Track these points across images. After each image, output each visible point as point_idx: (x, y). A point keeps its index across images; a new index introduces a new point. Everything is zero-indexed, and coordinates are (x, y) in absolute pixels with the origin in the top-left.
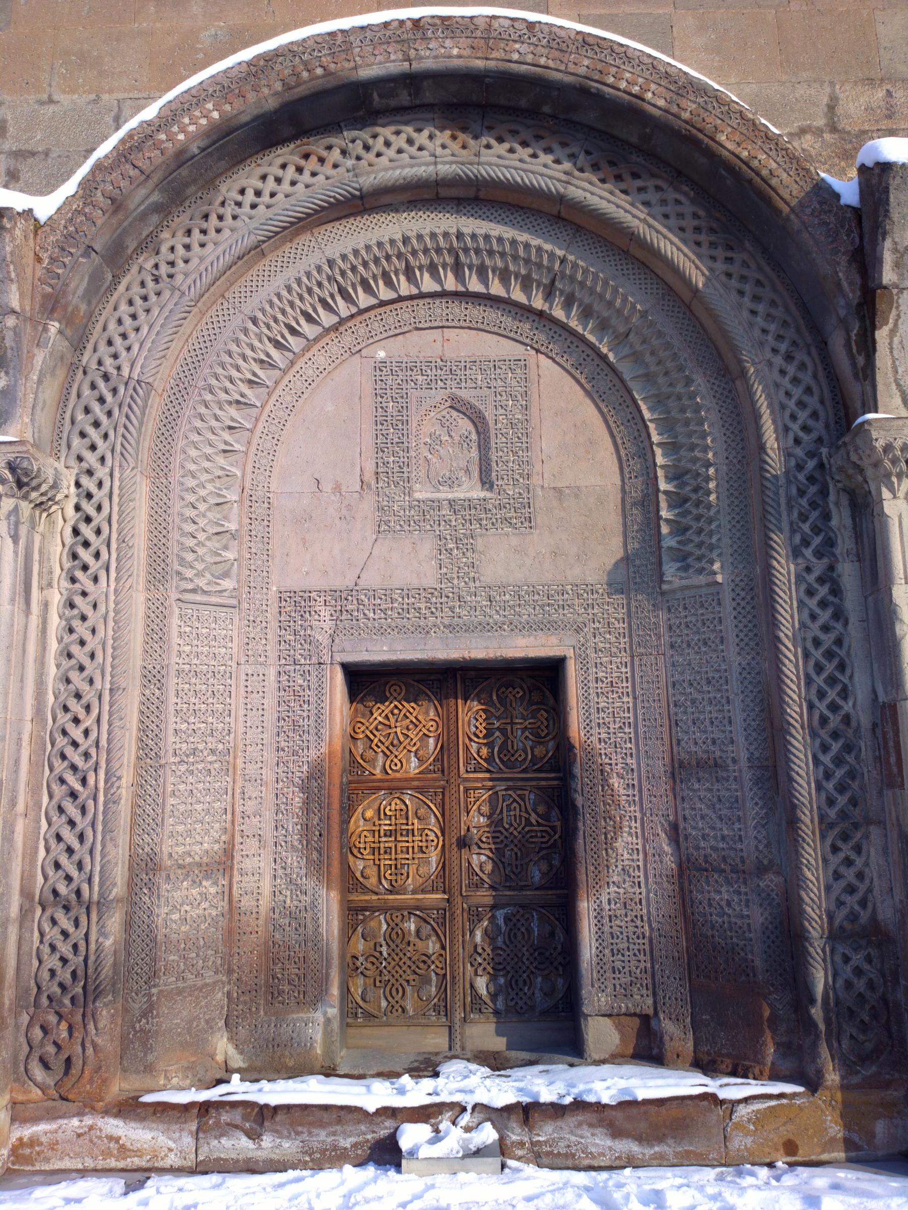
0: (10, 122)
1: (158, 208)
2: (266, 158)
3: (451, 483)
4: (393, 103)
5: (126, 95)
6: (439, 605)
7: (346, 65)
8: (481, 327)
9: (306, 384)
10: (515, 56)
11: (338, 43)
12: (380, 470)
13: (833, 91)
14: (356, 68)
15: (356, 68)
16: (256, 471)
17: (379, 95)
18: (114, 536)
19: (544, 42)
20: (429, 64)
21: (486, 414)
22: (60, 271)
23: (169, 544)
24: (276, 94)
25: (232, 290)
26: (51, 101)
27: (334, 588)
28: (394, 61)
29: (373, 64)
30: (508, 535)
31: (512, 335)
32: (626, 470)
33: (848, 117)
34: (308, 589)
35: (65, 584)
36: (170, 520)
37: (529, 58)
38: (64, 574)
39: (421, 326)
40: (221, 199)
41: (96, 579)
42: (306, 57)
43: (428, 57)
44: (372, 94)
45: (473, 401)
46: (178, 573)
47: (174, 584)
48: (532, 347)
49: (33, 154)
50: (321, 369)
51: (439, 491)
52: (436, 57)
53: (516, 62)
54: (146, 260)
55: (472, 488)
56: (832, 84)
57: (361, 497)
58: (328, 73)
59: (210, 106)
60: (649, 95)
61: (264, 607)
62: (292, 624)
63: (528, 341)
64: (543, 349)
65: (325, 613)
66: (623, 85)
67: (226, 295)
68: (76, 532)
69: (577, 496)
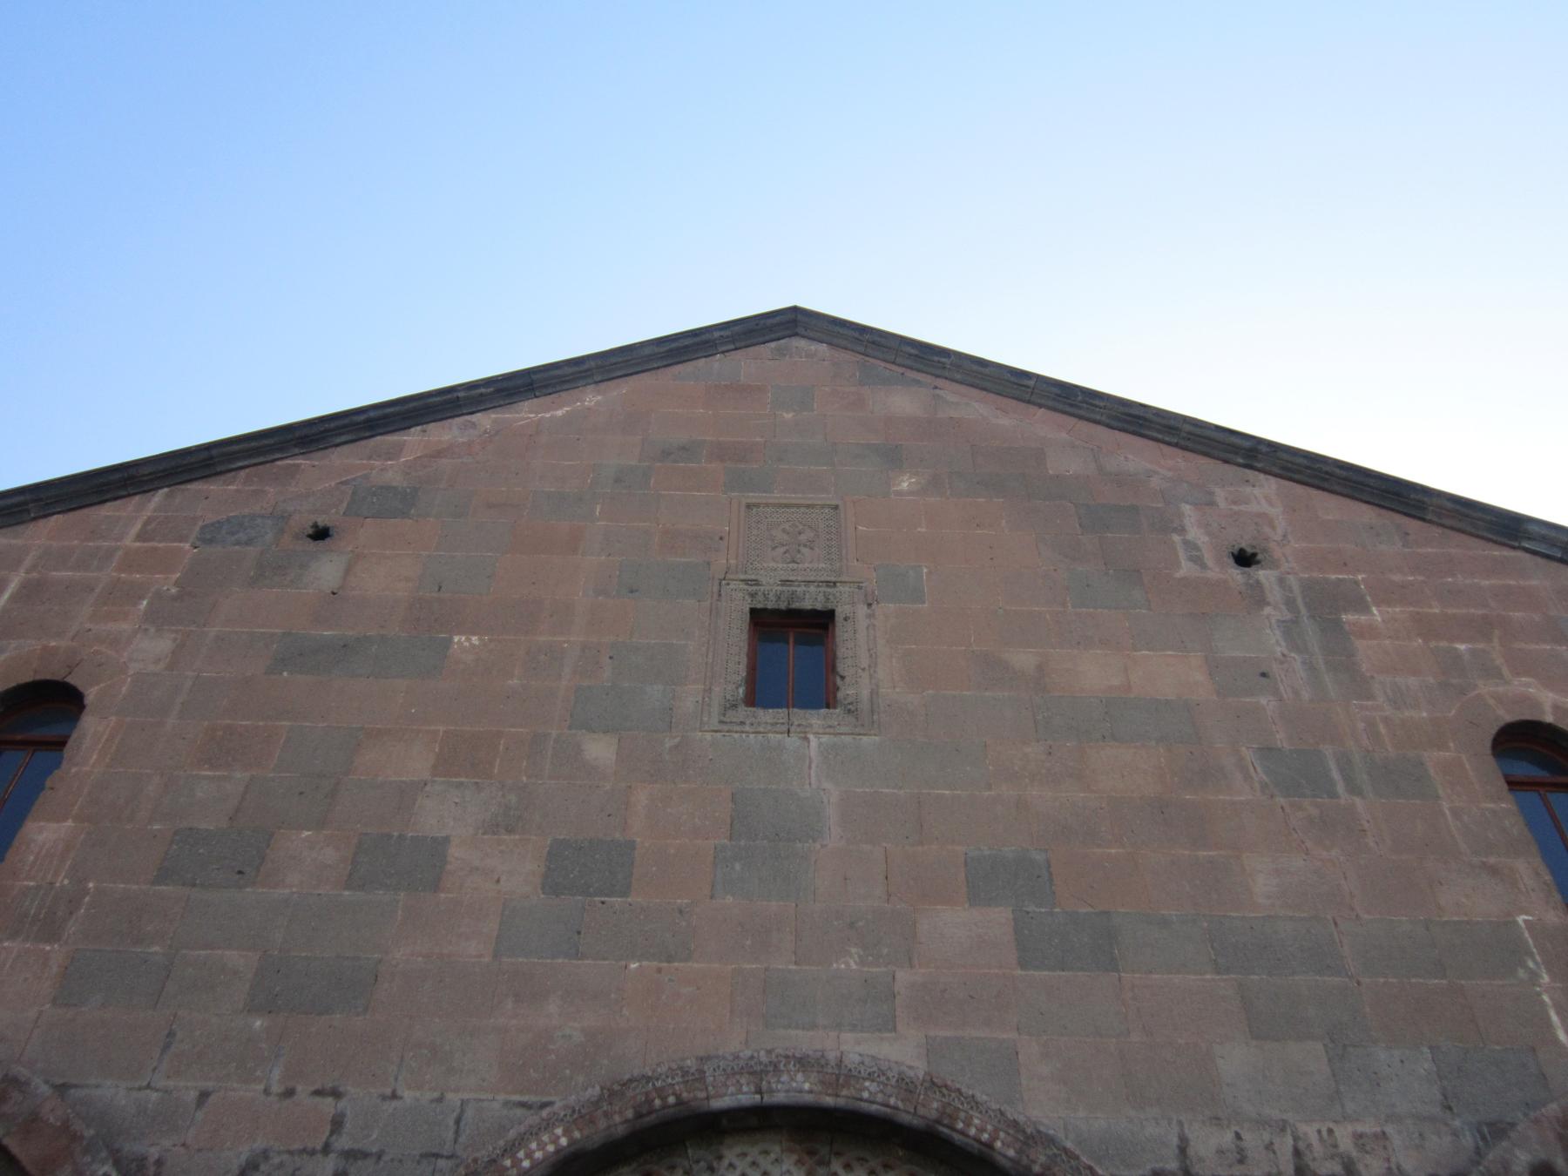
0: (348, 1113)
7: (702, 1095)
10: (866, 1095)
11: (692, 1070)
13: (1182, 1130)
14: (708, 1098)
15: (708, 1098)
19: (893, 1081)
20: (780, 1098)
24: (626, 1121)
26: (394, 1096)
28: (746, 1093)
29: (725, 1095)
33: (1201, 1160)
37: (880, 1098)
42: (659, 1084)
43: (779, 1091)
49: (366, 1155)
52: (787, 1091)
53: (866, 1101)
56: (1180, 1123)
58: (680, 1102)
59: (559, 1131)
60: (998, 1144)
66: (972, 1131)
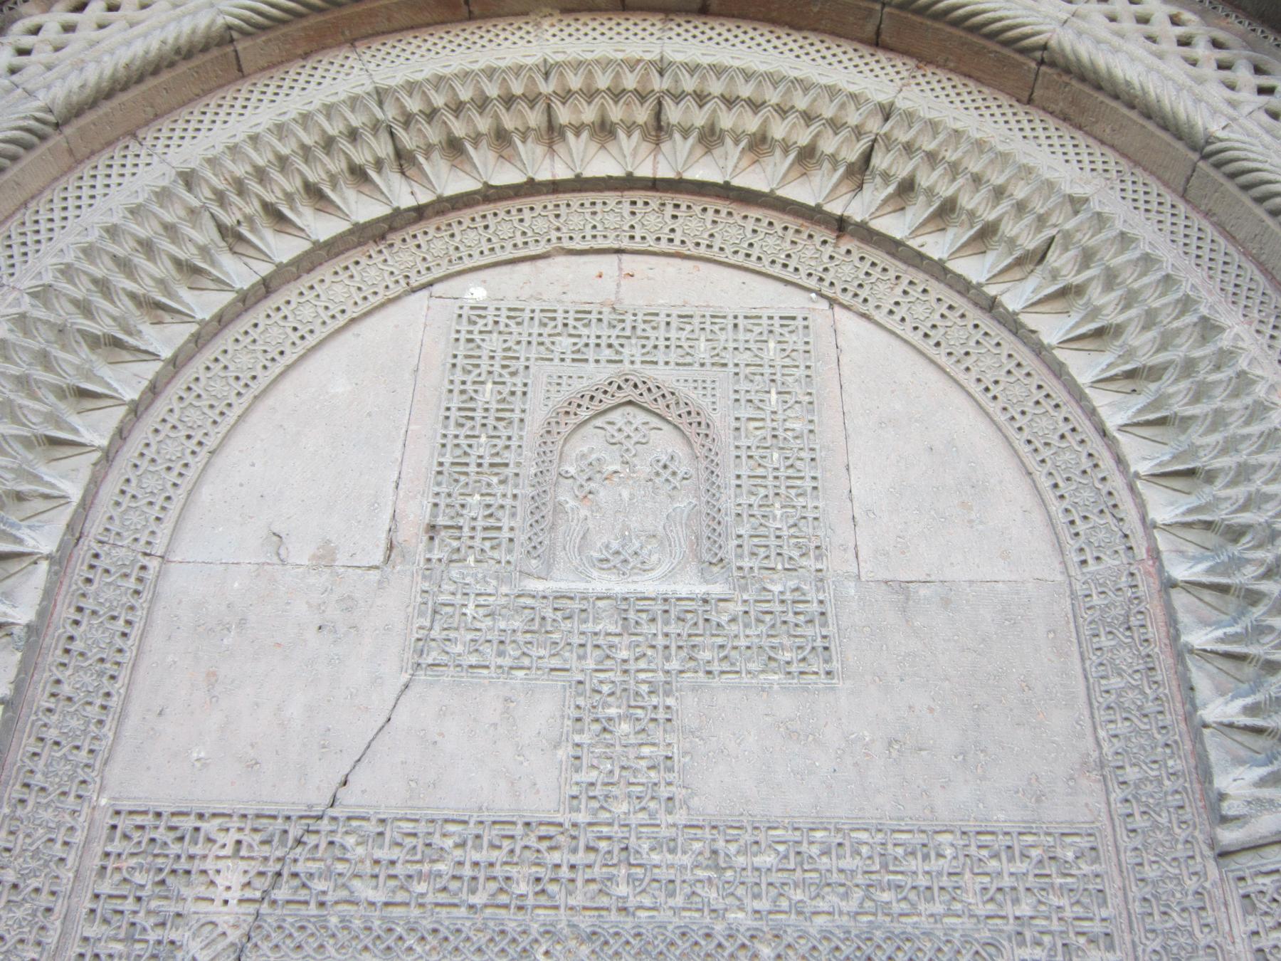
6: (565, 872)
8: (708, 254)
9: (294, 337)
12: (441, 521)
16: (126, 501)
21: (716, 417)
27: (269, 809)
31: (777, 270)
32: (1070, 545)
34: (197, 807)
45: (684, 390)
51: (588, 579)
55: (669, 576)
61: (58, 849)
62: (129, 905)
63: (812, 283)
64: (846, 299)
65: (231, 876)
67: (141, 134)
69: (946, 602)
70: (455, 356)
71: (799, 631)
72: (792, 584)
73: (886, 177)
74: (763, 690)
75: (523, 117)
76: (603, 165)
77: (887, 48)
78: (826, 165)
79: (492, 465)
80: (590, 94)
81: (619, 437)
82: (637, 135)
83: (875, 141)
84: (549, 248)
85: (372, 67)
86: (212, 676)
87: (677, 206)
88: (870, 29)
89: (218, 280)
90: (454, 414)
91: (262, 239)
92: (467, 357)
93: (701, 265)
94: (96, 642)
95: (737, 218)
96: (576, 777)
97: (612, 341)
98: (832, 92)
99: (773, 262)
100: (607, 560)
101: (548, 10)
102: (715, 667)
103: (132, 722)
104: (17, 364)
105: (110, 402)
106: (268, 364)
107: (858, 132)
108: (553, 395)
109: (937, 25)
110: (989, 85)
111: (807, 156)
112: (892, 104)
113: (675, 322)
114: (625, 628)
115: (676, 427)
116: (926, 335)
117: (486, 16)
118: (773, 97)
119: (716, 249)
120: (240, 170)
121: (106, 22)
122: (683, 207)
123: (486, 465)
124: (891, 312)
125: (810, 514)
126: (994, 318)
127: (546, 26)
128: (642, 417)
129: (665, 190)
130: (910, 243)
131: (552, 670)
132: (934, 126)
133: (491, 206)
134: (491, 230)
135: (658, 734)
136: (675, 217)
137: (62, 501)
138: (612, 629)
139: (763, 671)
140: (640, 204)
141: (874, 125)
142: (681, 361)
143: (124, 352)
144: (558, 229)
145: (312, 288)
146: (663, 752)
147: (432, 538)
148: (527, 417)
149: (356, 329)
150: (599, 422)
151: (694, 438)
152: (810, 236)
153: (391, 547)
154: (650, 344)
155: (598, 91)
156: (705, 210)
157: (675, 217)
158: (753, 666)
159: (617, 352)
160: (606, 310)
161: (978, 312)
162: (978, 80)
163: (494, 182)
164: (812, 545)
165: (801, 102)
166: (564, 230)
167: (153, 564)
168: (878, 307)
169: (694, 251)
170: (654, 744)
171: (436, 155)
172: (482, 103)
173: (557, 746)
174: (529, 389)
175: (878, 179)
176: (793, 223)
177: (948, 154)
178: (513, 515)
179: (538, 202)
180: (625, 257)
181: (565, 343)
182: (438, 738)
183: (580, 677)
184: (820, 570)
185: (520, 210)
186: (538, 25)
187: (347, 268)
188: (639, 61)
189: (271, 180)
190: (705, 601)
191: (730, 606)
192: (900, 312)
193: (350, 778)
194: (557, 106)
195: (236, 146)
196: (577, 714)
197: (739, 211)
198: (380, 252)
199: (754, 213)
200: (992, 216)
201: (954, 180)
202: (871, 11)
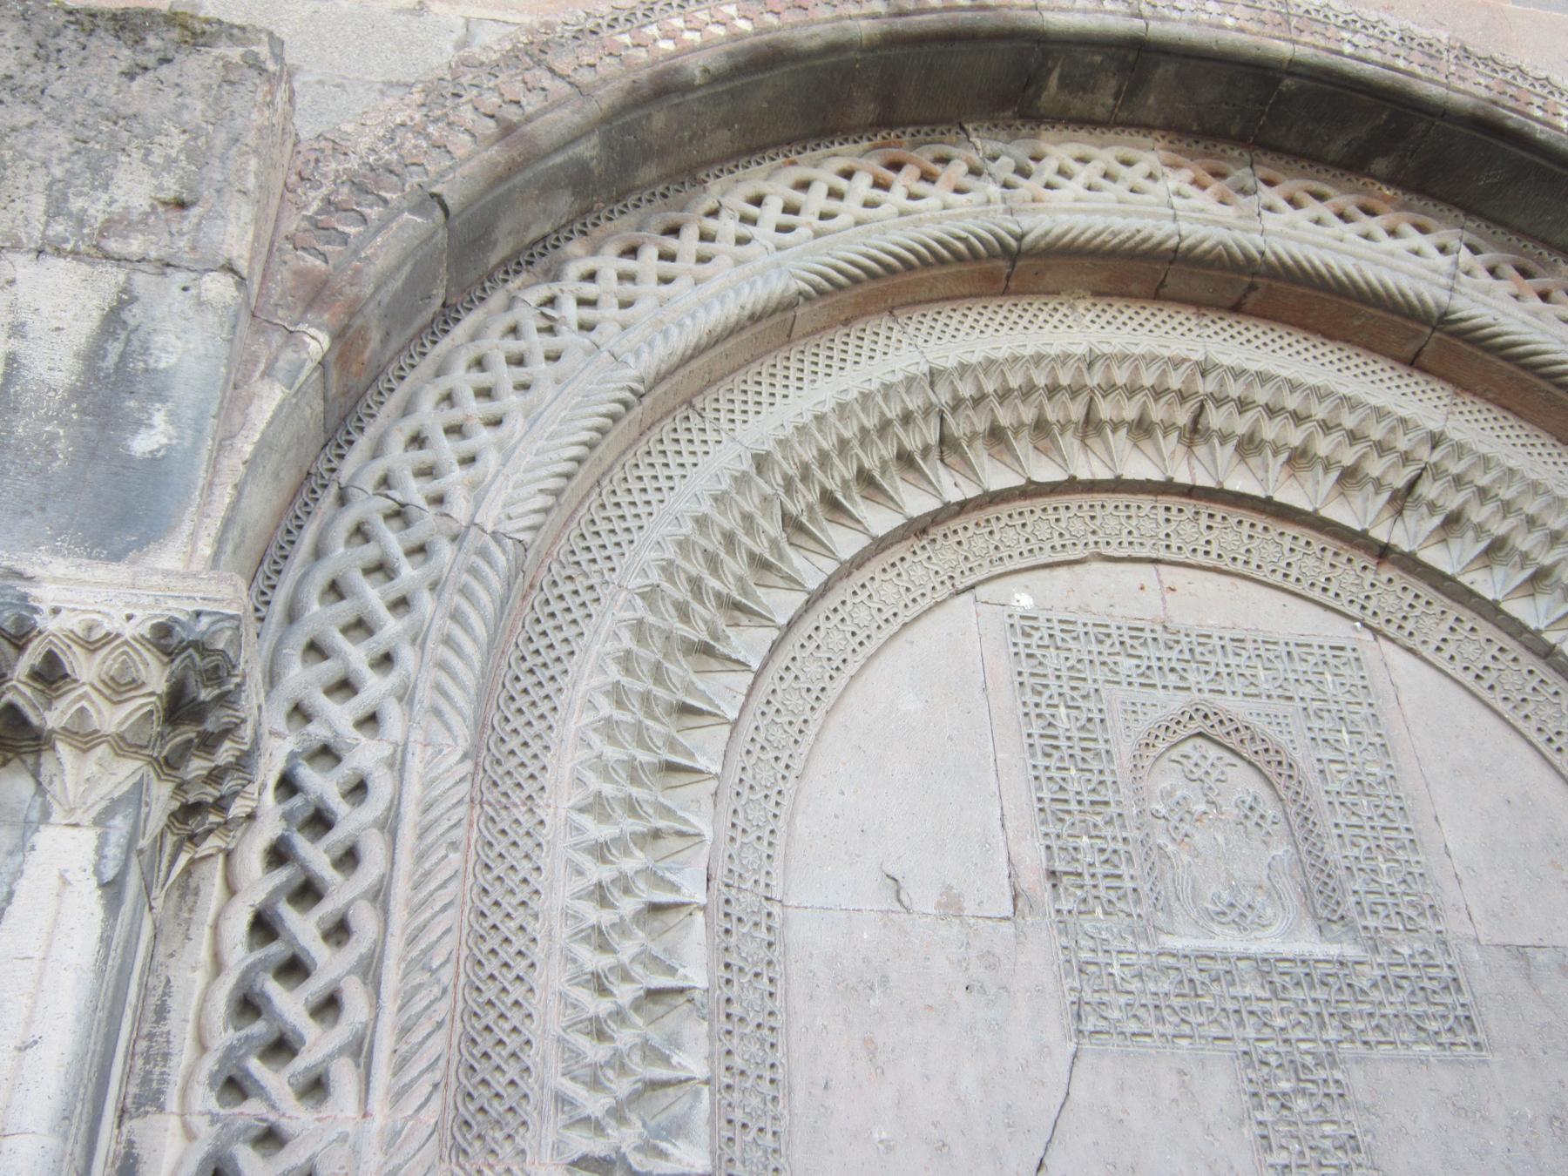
1: (580, 180)
2: (808, 153)
3: (1236, 915)
4: (1078, 105)
5: (485, 13)
12: (1060, 866)
17: (1061, 78)
18: (395, 946)
21: (1297, 755)
22: (352, 230)
23: (534, 1004)
25: (711, 393)
30: (1423, 1062)
31: (1316, 594)
35: (205, 1099)
36: (534, 927)
38: (210, 1063)
39: (1109, 551)
40: (710, 204)
41: (316, 1087)
44: (1050, 71)
45: (1259, 725)
46: (562, 1100)
47: (550, 1139)
48: (1365, 625)
50: (888, 614)
51: (1211, 935)
54: (525, 286)
57: (1020, 936)
63: (1354, 610)
64: (1391, 630)
67: (698, 404)
68: (264, 927)
70: (1020, 674)
71: (1437, 999)
72: (1418, 946)
73: (1432, 507)
74: (1422, 1062)
75: (1066, 409)
76: (1138, 467)
77: (1424, 370)
78: (1370, 488)
79: (1093, 803)
80: (1132, 390)
81: (1198, 773)
82: (1174, 436)
83: (1424, 469)
84: (1086, 553)
85: (920, 342)
86: (868, 1042)
87: (1211, 516)
88: (1411, 348)
89: (790, 578)
90: (1039, 743)
91: (822, 530)
92: (1033, 675)
93: (1238, 582)
94: (751, 1004)
95: (1273, 534)
96: (1270, 1159)
97: (1174, 664)
98: (1380, 414)
99: (1313, 585)
100: (1224, 913)
101: (1082, 293)
102: (1372, 1037)
103: (799, 1096)
104: (639, 679)
105: (712, 720)
106: (834, 673)
107: (1406, 458)
108: (1132, 724)
109: (1488, 357)
110: (1529, 421)
111: (1349, 477)
112: (1442, 433)
113: (1230, 647)
114: (1274, 992)
115: (1250, 763)
116: (1478, 677)
117: (1020, 293)
118: (1320, 411)
119: (1253, 566)
120: (809, 454)
121: (669, 275)
122: (1218, 518)
123: (1087, 803)
124: (1438, 649)
125: (1416, 870)
126: (1548, 664)
127: (1081, 310)
128: (1213, 752)
129: (1199, 498)
130: (1461, 579)
131: (1216, 1038)
132: (1485, 462)
133: (1028, 502)
134: (1029, 529)
135: (1336, 1112)
136: (1209, 528)
137: (697, 839)
138: (1261, 993)
139: (1416, 1042)
140: (1174, 510)
141: (1424, 453)
142: (1247, 691)
143: (712, 661)
144: (1094, 532)
145: (863, 586)
146: (1345, 1131)
147: (1054, 886)
148: (1114, 751)
149: (909, 634)
150: (1174, 754)
151: (1274, 779)
152: (1349, 560)
153: (1015, 898)
154: (1213, 670)
155: (1142, 388)
156: (1240, 522)
157: (1209, 528)
158: (1406, 1037)
159: (1182, 678)
160: (1158, 628)
161: (1532, 658)
162: (1517, 414)
163: (1035, 478)
164: (1426, 905)
165: (1349, 421)
166: (1101, 533)
167: (776, 909)
168: (1424, 642)
169: (1231, 567)
170: (1333, 1122)
171: (979, 444)
172: (1028, 391)
173: (1241, 1123)
174: (1106, 716)
175: (1424, 509)
176: (1332, 545)
177: (1501, 492)
178: (1130, 860)
179: (1074, 500)
180: (1161, 568)
181: (1126, 664)
182: (1122, 1116)
183: (1244, 1047)
184: (1439, 932)
185: (1056, 509)
186: (1072, 307)
187: (893, 565)
188: (1184, 360)
189: (832, 465)
190: (1342, 964)
191: (1365, 968)
192: (1449, 649)
193: (1046, 1161)
194: (1098, 399)
195: (805, 426)
196: (1251, 1088)
197: (1277, 527)
198: (923, 548)
199: (1291, 530)
200: (1547, 560)
201: (1504, 517)
202: (1417, 334)
